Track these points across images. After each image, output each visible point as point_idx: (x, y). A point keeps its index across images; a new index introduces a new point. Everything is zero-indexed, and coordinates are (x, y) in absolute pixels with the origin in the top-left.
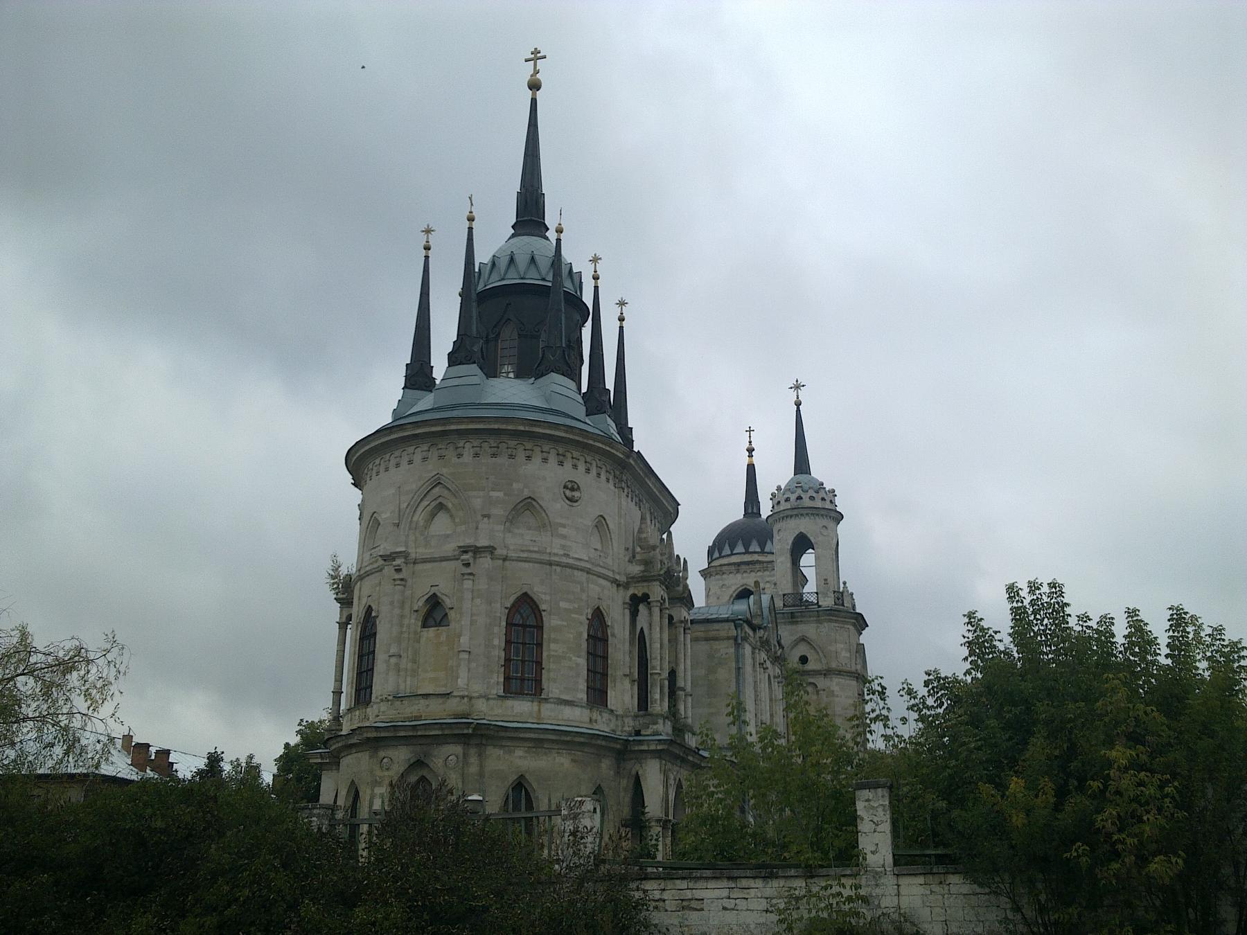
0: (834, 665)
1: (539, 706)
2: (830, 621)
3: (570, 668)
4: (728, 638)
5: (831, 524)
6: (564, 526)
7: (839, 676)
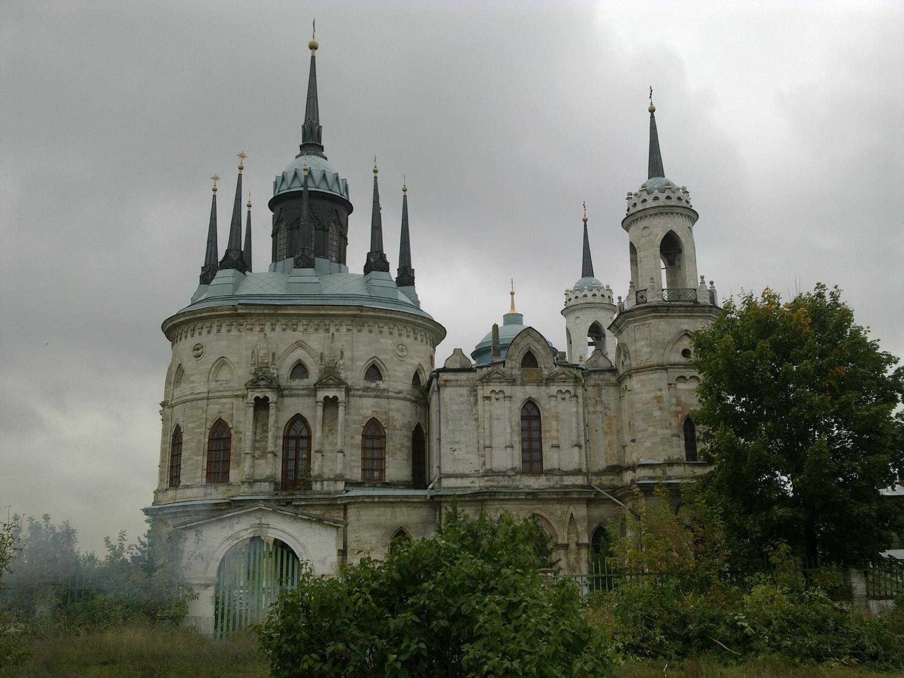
0: (634, 365)
2: (630, 322)
3: (192, 464)
6: (193, 375)
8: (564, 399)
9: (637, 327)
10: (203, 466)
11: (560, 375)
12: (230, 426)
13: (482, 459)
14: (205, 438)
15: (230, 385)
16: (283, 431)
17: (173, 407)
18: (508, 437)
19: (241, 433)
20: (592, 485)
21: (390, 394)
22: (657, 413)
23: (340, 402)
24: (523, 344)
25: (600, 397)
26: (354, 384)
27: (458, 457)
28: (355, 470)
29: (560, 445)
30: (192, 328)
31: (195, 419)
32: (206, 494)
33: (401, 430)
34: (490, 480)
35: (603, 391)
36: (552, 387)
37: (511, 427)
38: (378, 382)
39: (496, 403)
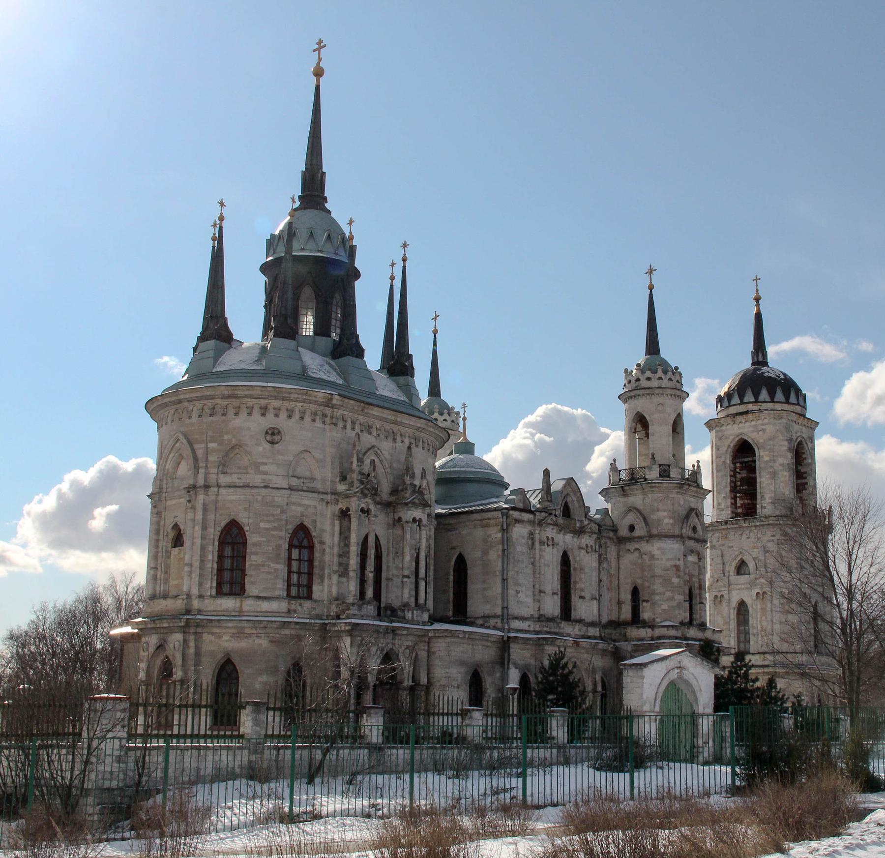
0: (655, 531)
1: (242, 601)
2: (652, 492)
4: (497, 525)
6: (266, 464)
12: (314, 534)
13: (537, 604)
15: (313, 485)
19: (324, 543)
22: (675, 580)
32: (289, 611)
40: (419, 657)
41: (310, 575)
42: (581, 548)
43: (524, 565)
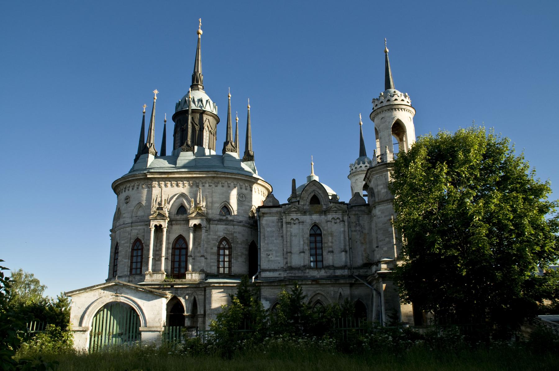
0: (377, 200)
3: (123, 264)
5: (387, 114)
6: (124, 213)
7: (380, 206)
8: (336, 223)
9: (378, 177)
10: (128, 265)
11: (333, 208)
12: (143, 242)
13: (285, 260)
14: (129, 249)
16: (172, 245)
17: (115, 232)
18: (302, 246)
20: (353, 275)
21: (234, 223)
23: (202, 227)
24: (311, 190)
25: (359, 222)
26: (213, 217)
27: (271, 259)
28: (213, 268)
29: (334, 251)
30: (125, 187)
31: (125, 238)
33: (241, 244)
34: (290, 273)
35: (361, 218)
36: (328, 216)
37: (304, 240)
38: (227, 216)
39: (294, 226)
40: (197, 299)
41: (141, 262)
42: (327, 221)
43: (274, 239)
